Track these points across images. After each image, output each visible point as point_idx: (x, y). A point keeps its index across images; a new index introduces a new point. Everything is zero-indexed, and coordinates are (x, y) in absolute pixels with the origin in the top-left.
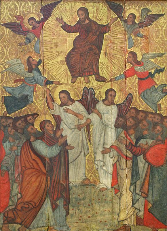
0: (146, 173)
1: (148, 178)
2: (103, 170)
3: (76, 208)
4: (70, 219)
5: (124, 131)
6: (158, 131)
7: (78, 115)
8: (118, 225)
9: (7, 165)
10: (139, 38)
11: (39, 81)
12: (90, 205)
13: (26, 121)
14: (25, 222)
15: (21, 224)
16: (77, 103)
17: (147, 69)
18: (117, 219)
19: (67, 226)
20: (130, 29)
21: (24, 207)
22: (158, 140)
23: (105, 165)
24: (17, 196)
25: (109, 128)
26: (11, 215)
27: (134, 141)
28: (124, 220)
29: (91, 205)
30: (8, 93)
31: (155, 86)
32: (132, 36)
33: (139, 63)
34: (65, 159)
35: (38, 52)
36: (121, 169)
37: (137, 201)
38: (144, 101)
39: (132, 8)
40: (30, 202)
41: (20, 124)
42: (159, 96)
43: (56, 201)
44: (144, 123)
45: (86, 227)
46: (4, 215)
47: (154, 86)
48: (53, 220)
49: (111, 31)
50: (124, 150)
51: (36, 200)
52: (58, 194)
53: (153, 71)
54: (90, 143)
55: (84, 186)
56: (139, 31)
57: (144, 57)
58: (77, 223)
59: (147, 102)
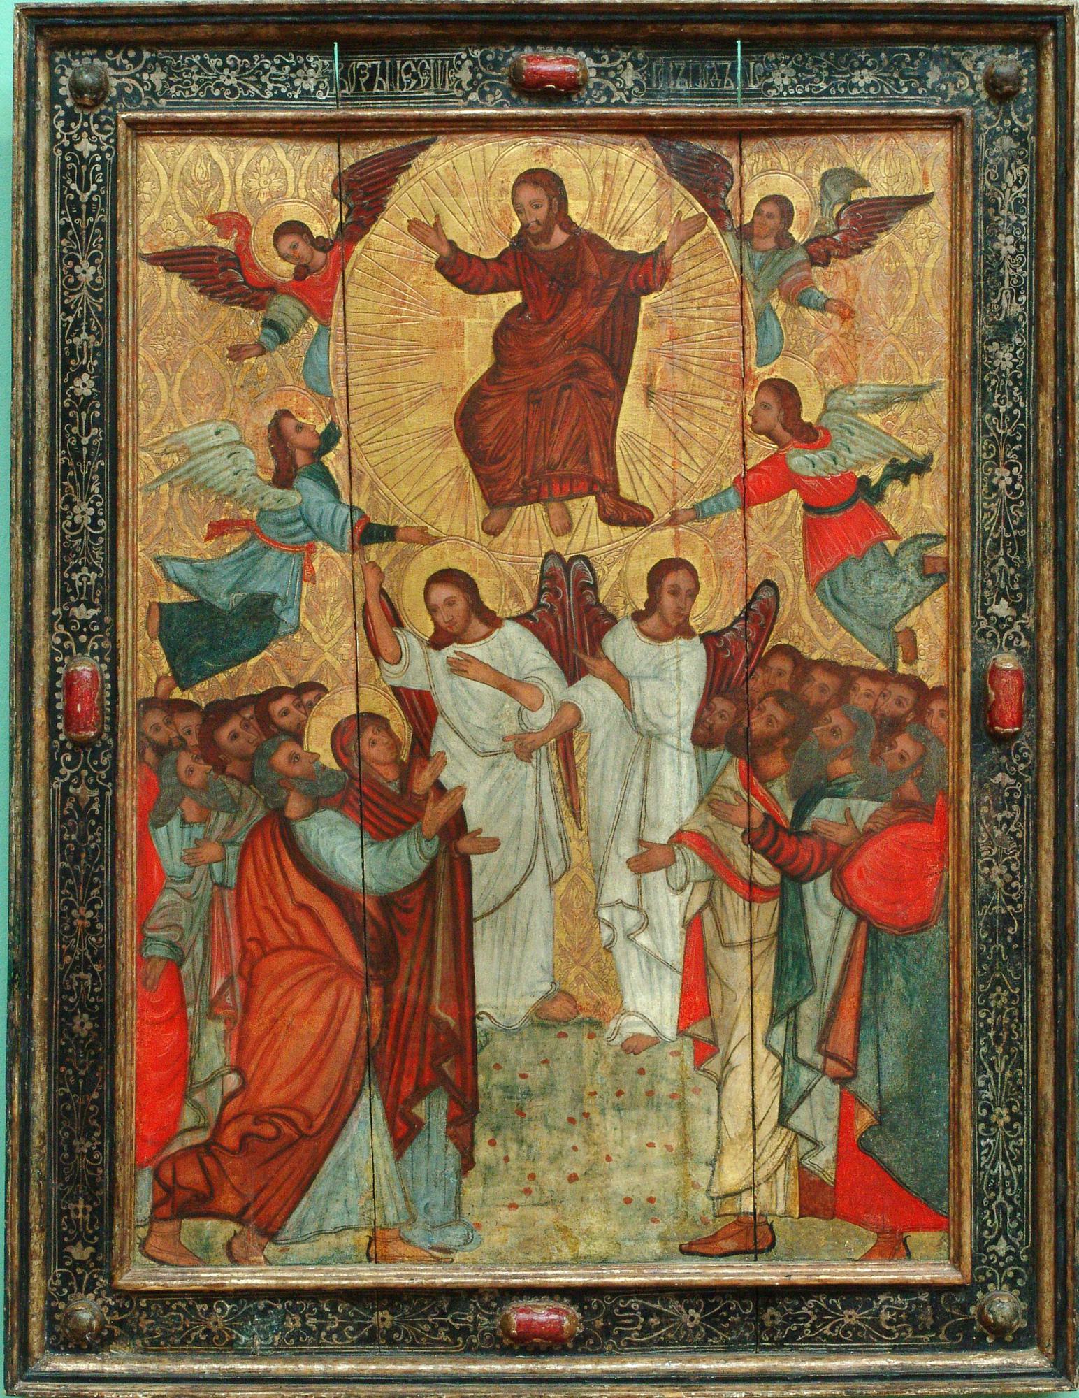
0: (845, 964)
1: (853, 987)
2: (639, 947)
3: (509, 1134)
4: (481, 1190)
5: (736, 761)
6: (902, 758)
7: (519, 688)
8: (710, 1217)
9: (174, 934)
10: (810, 315)
11: (326, 527)
12: (577, 1118)
13: (264, 720)
14: (261, 1209)
15: (239, 1218)
16: (511, 630)
17: (850, 462)
18: (705, 1186)
19: (467, 1225)
20: (765, 272)
21: (259, 1136)
22: (902, 804)
23: (646, 924)
24: (219, 1082)
25: (668, 750)
26: (191, 1176)
27: (789, 810)
28: (739, 1193)
29: (580, 1119)
30: (180, 585)
31: (888, 543)
32: (774, 303)
33: (810, 436)
34: (454, 901)
35: (321, 388)
36: (725, 946)
37: (802, 1098)
38: (834, 614)
39: (780, 170)
40: (283, 1111)
41: (234, 736)
42: (905, 589)
43: (413, 1105)
44: (835, 722)
45: (559, 1229)
46: (157, 1175)
47: (881, 540)
48: (399, 1196)
49: (675, 282)
50: (739, 854)
51: (313, 1102)
52: (420, 1071)
53: (875, 474)
54: (578, 822)
55: (546, 1027)
56: (808, 280)
57: (834, 403)
58: (513, 1206)
59: (848, 619)
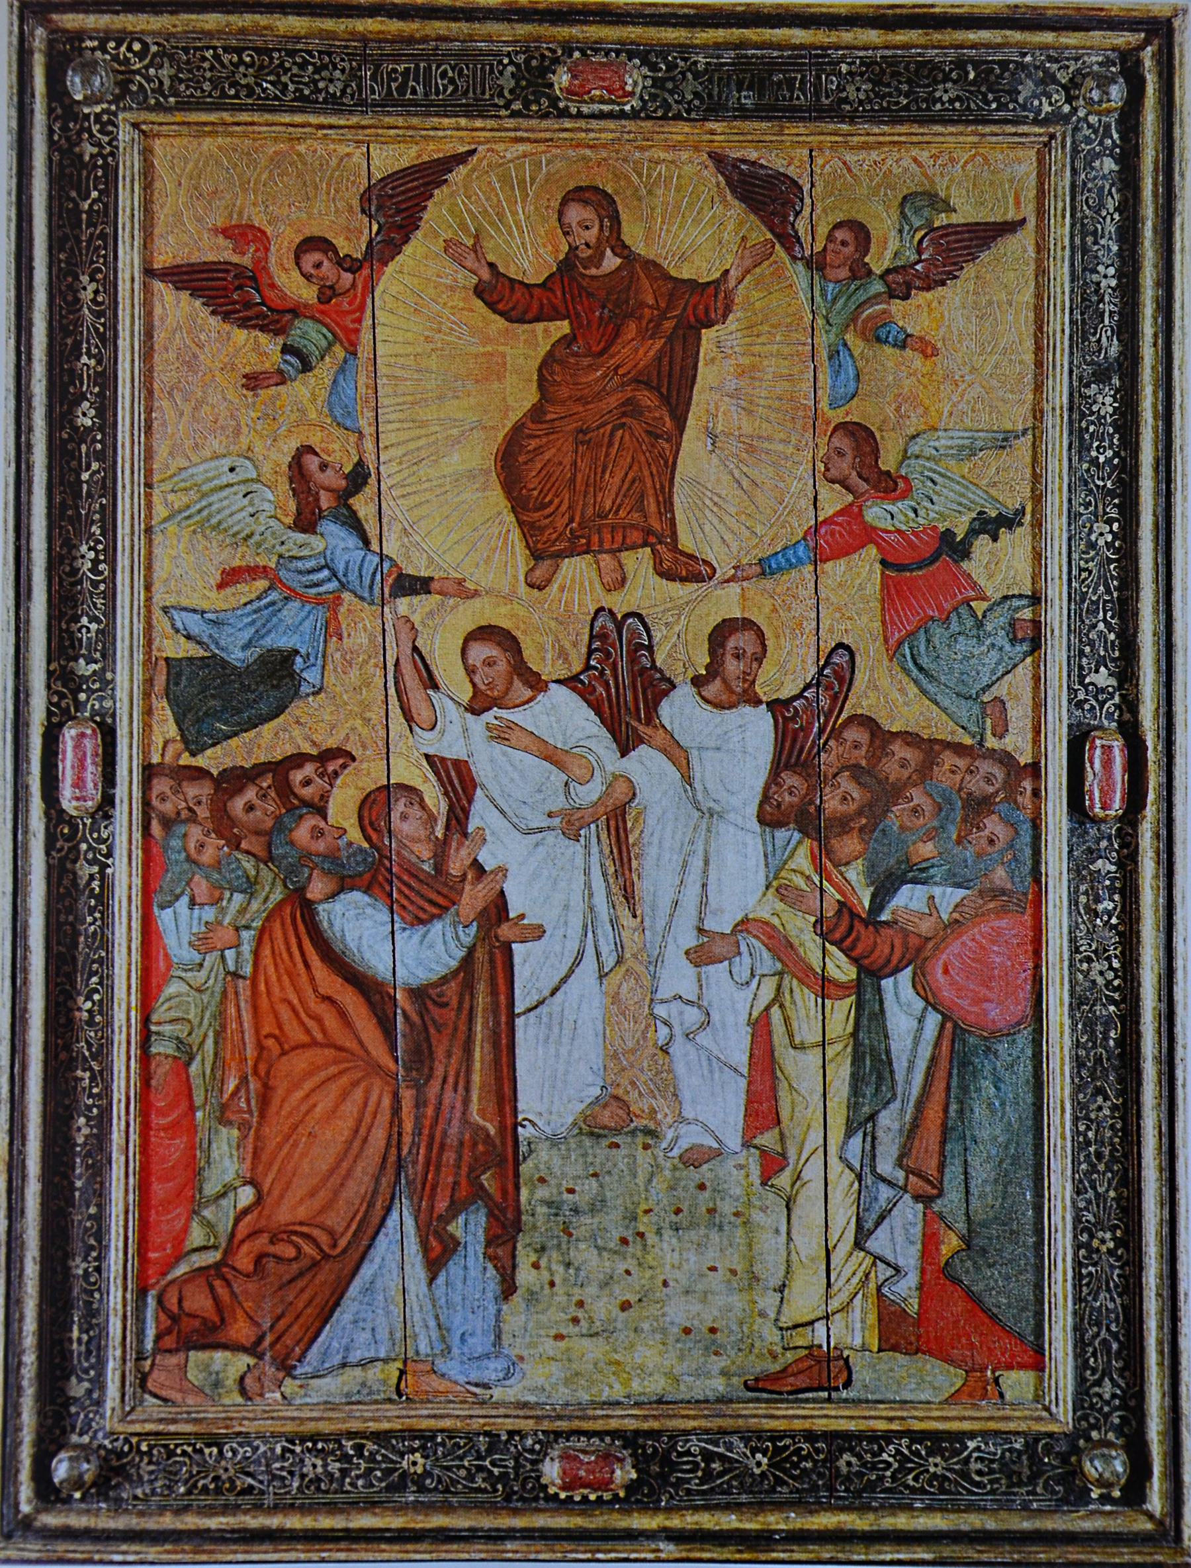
0: (929, 1068)
3: (555, 1255)
5: (807, 842)
7: (566, 758)
8: (779, 1350)
9: (181, 1030)
11: (353, 577)
12: (630, 1239)
13: (284, 790)
15: (253, 1350)
16: (560, 694)
17: (932, 515)
18: (773, 1316)
24: (231, 1195)
25: (732, 829)
26: (199, 1302)
28: (812, 1323)
30: (188, 637)
35: (348, 423)
36: (795, 1048)
37: (882, 1218)
40: (305, 1229)
41: (250, 808)
43: (448, 1223)
44: (916, 802)
47: (967, 602)
48: (432, 1323)
50: (810, 947)
55: (599, 1136)
57: (914, 449)
58: (559, 1337)
59: (932, 689)
